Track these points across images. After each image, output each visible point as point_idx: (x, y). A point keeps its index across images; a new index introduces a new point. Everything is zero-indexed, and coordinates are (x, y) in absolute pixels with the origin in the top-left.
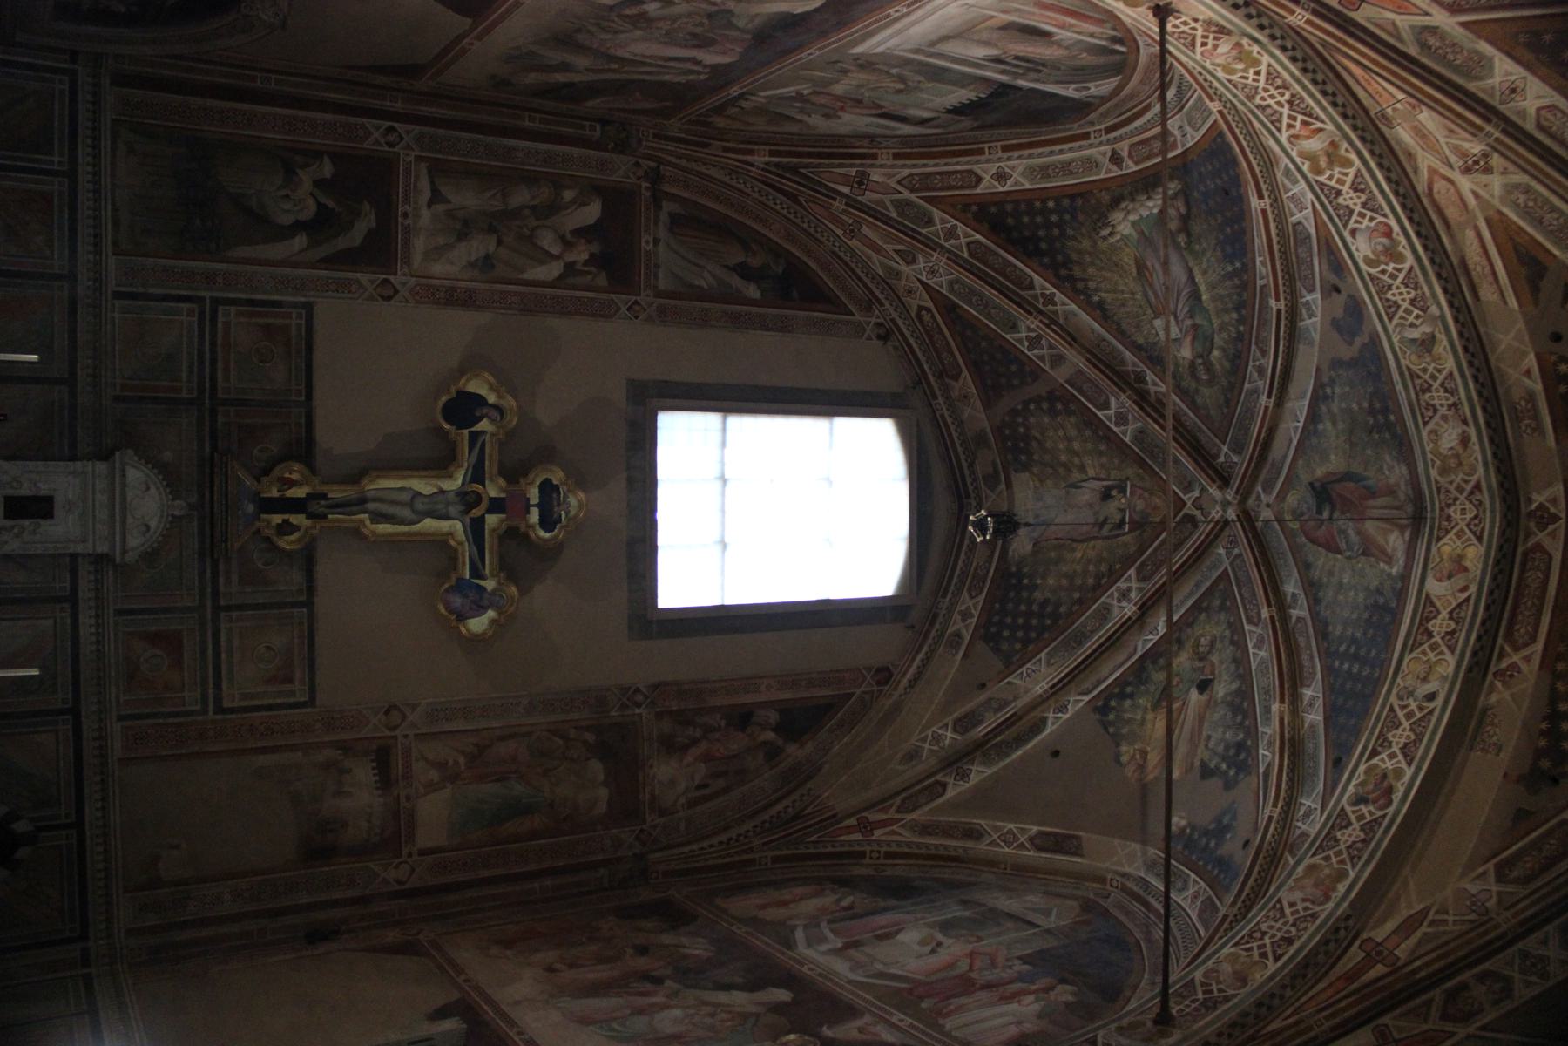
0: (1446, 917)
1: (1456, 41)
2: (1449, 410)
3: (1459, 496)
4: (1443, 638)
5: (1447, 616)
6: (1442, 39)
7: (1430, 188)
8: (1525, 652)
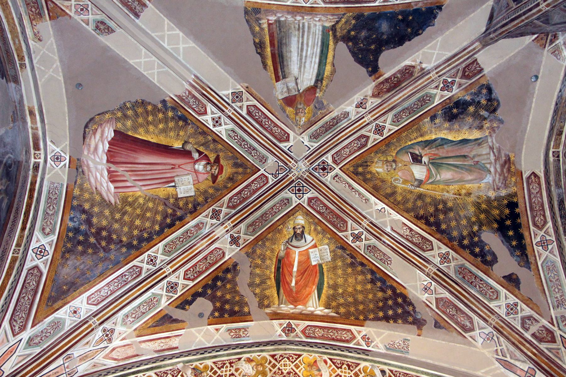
0: (499, 351)
1: (40, 331)
2: (233, 367)
3: (277, 367)
4: (352, 371)
5: (340, 370)
6: (37, 336)
7: (115, 359)
8: (356, 333)
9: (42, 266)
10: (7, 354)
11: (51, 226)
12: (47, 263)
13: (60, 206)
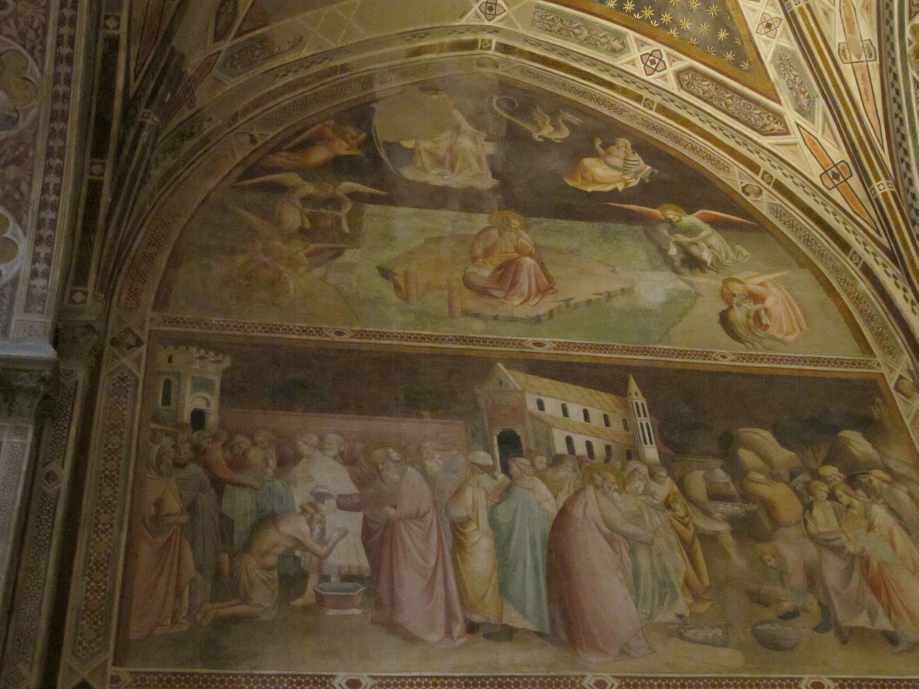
1: (789, 91)
6: (797, 99)
9: (678, 66)
10: (816, 150)
11: (609, 37)
12: (673, 56)
13: (573, 16)
